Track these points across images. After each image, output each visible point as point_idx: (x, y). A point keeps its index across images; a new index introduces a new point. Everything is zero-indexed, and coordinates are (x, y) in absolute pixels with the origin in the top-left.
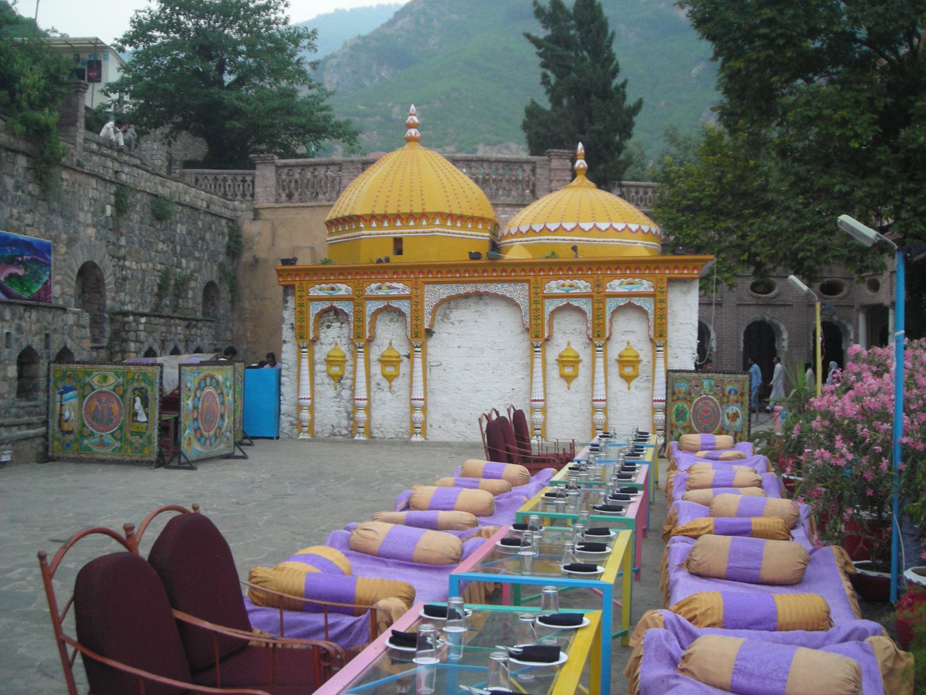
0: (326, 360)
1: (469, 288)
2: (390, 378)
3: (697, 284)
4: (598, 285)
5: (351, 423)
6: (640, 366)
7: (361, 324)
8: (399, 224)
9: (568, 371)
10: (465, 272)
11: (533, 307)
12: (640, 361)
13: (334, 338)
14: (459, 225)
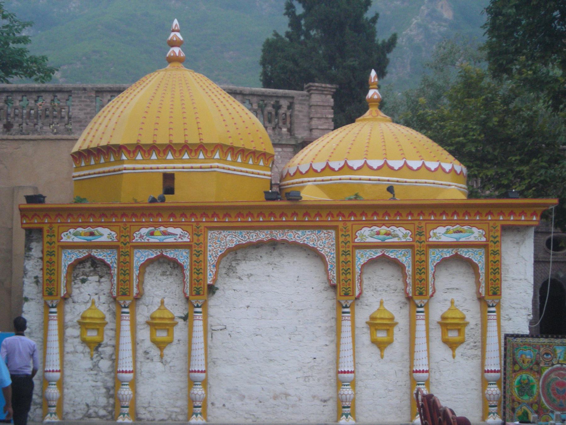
0: (79, 323)
1: (263, 236)
2: (161, 345)
3: (531, 233)
4: (420, 233)
5: (112, 401)
6: (467, 330)
7: (127, 277)
8: (170, 156)
9: (381, 335)
10: (258, 216)
11: (342, 258)
12: (467, 324)
13: (90, 296)
14: (239, 160)
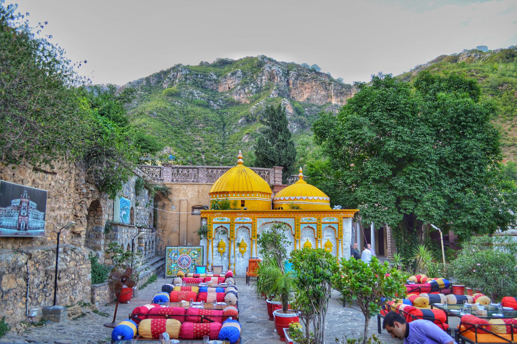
1: (273, 220)
